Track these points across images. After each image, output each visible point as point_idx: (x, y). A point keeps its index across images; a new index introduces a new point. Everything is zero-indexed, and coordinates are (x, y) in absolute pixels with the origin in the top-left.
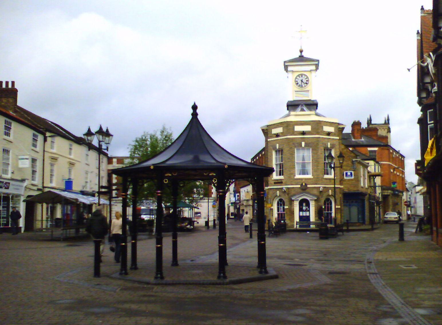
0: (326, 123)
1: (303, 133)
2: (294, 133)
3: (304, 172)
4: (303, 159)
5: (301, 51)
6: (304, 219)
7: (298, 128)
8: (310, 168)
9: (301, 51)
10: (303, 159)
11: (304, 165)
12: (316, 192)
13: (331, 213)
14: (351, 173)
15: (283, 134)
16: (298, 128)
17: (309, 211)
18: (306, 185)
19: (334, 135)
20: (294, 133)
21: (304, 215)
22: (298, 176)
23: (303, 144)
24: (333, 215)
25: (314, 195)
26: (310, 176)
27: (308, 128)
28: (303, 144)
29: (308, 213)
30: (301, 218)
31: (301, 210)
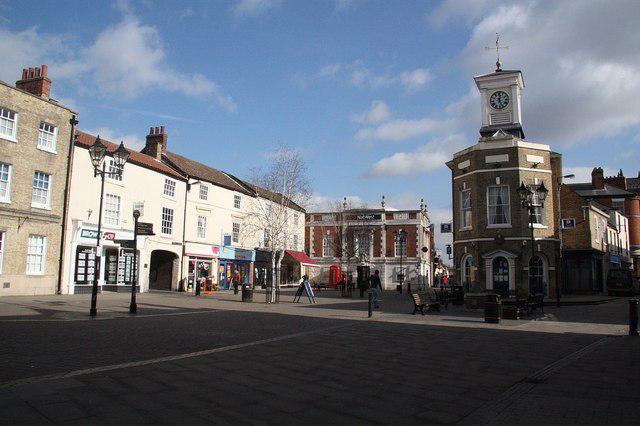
0: (530, 151)
1: (498, 165)
2: (484, 165)
3: (499, 219)
4: (499, 201)
5: (498, 65)
6: (501, 287)
7: (489, 159)
8: (508, 214)
9: (498, 65)
10: (499, 201)
11: (499, 210)
12: (516, 247)
13: (541, 278)
14: (572, 221)
15: (470, 168)
16: (489, 159)
17: (508, 274)
18: (502, 237)
19: (544, 167)
20: (484, 165)
21: (501, 280)
22: (491, 226)
23: (498, 180)
24: (545, 280)
25: (513, 252)
26: (508, 225)
27: (505, 158)
28: (498, 180)
29: (506, 277)
30: (496, 284)
31: (495, 272)
